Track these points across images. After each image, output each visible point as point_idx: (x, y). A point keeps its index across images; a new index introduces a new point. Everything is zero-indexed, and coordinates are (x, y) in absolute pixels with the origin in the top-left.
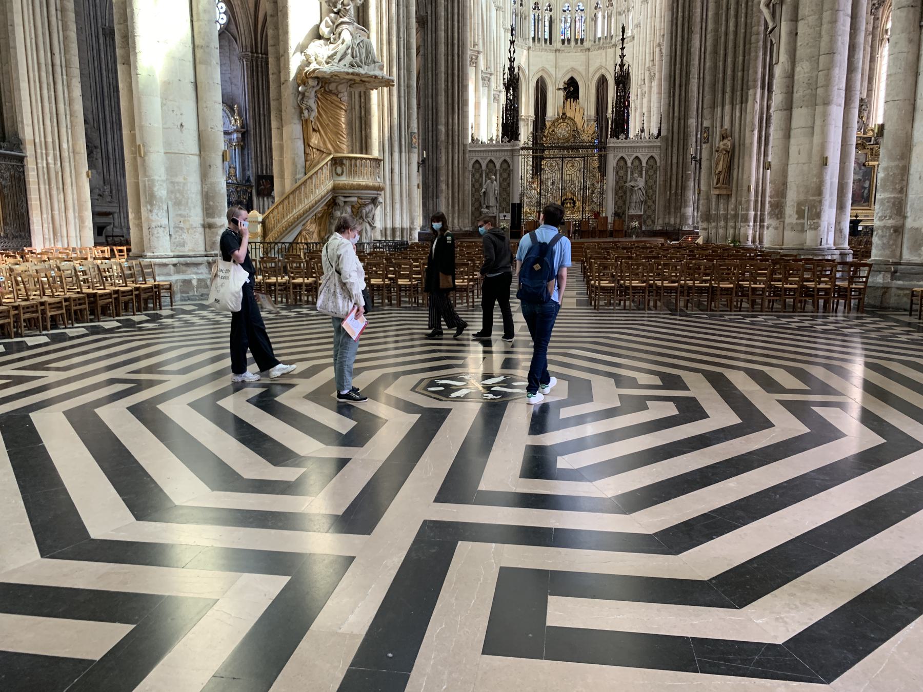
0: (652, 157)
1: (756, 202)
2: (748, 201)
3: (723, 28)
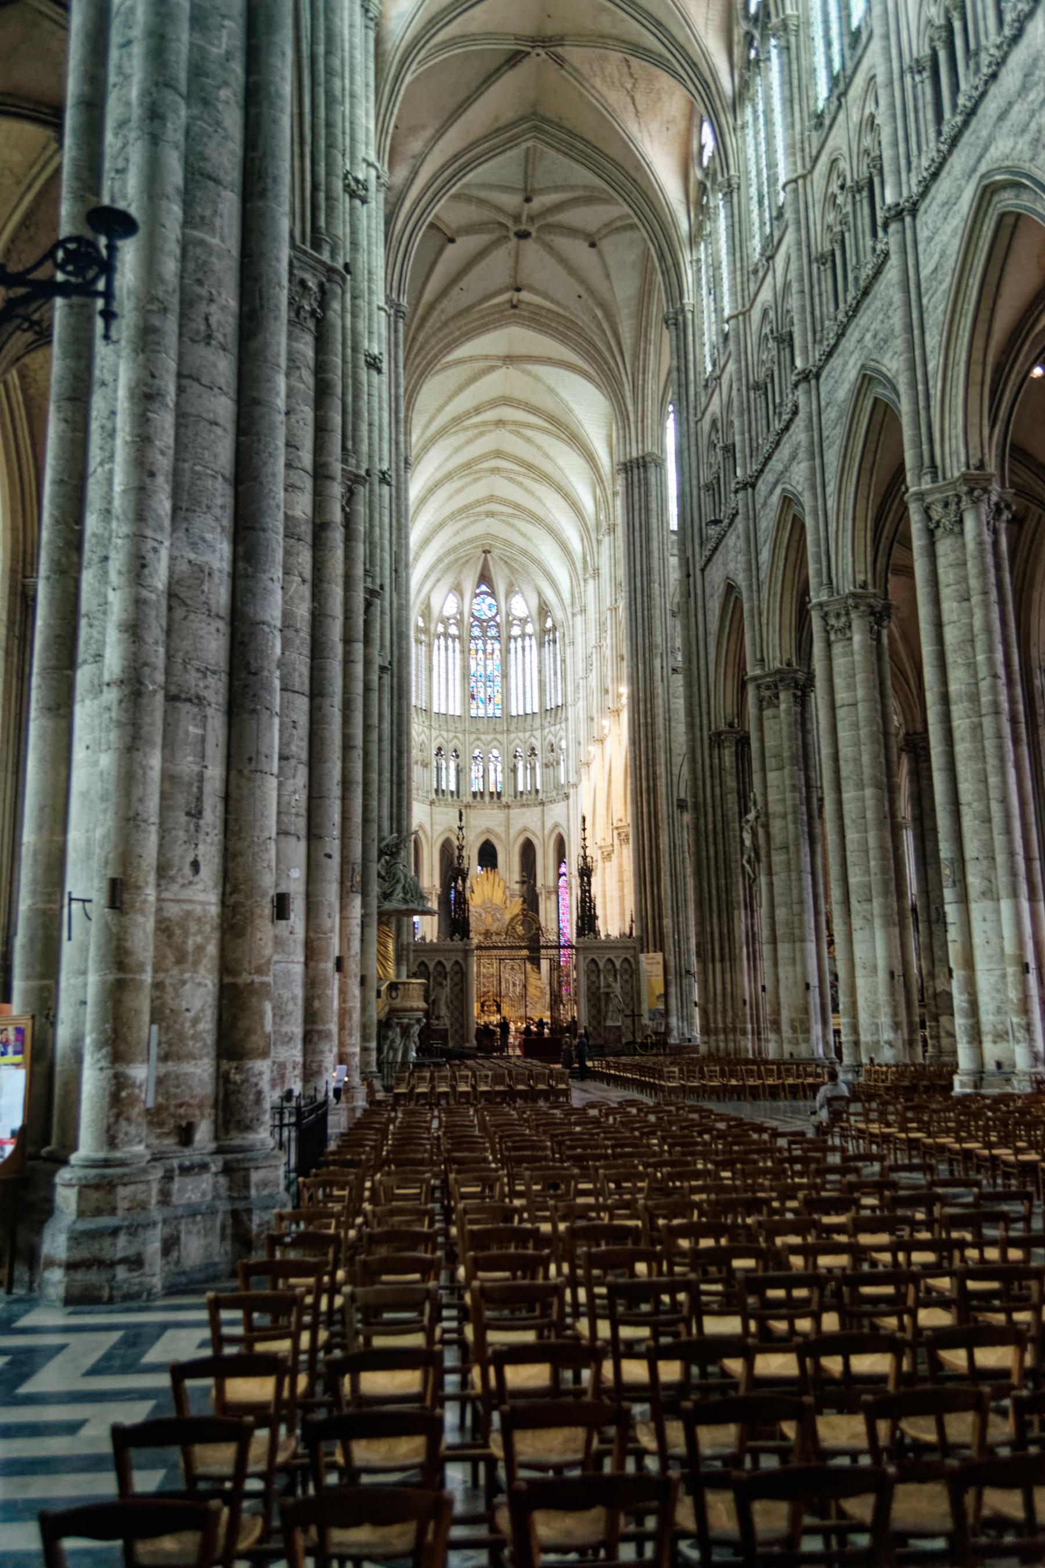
0: (626, 959)
1: (752, 1015)
2: (744, 1015)
3: (704, 853)
